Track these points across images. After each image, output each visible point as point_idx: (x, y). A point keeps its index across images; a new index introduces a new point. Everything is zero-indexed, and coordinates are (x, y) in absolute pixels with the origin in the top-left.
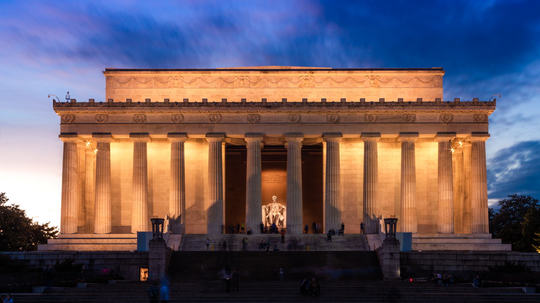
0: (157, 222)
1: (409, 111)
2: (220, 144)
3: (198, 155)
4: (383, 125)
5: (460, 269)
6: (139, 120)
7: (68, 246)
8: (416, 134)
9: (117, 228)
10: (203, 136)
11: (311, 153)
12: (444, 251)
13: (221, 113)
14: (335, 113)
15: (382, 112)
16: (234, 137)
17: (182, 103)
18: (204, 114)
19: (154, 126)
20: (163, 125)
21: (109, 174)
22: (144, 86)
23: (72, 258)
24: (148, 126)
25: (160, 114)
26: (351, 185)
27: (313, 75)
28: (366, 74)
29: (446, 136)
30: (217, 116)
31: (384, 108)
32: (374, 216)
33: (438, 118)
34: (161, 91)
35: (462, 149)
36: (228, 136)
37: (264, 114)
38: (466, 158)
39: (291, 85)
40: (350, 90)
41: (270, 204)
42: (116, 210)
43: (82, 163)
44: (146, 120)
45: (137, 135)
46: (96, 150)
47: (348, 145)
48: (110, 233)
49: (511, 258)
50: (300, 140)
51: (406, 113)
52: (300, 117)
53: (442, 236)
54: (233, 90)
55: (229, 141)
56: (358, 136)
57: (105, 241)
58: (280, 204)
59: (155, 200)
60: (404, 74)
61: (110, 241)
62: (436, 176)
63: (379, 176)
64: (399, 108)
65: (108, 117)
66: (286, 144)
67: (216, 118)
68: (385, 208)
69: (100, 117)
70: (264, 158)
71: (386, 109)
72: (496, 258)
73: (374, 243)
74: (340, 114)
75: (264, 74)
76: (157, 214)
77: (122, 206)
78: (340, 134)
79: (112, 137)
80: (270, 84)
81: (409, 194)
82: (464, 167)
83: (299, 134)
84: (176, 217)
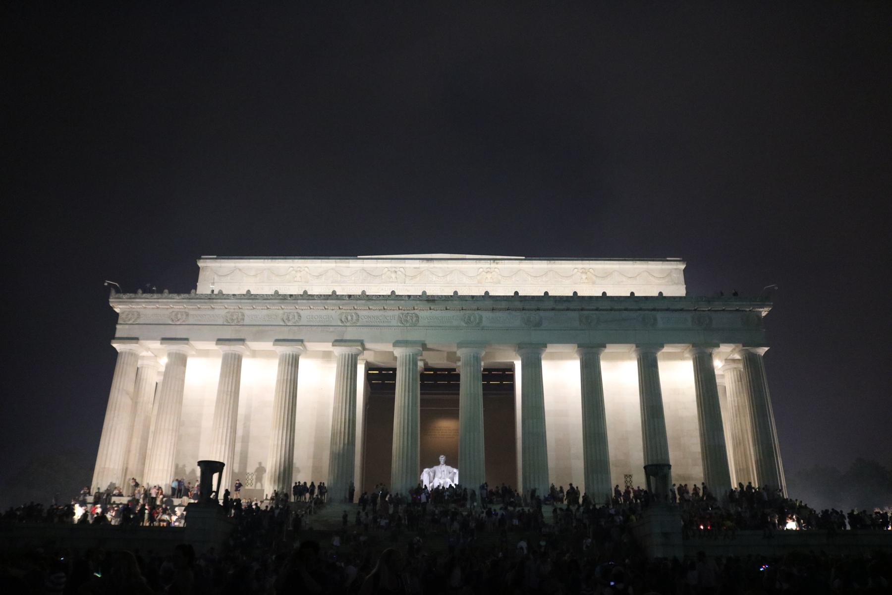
10: (328, 347)
13: (358, 312)
18: (333, 313)
19: (255, 329)
25: (265, 312)
28: (574, 266)
30: (352, 316)
36: (368, 345)
37: (425, 314)
41: (435, 468)
52: (481, 318)
55: (369, 356)
58: (449, 467)
65: (187, 315)
67: (349, 318)
69: (176, 315)
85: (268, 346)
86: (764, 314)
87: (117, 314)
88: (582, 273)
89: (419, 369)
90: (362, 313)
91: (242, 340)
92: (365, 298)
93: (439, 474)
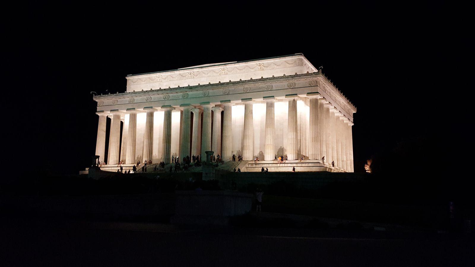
1: (269, 84)
6: (131, 101)
13: (169, 94)
15: (252, 85)
18: (161, 96)
22: (143, 83)
24: (135, 104)
27: (227, 67)
29: (291, 97)
30: (167, 96)
39: (215, 74)
52: (209, 92)
65: (117, 101)
67: (166, 97)
78: (229, 101)
80: (204, 75)
83: (208, 103)
85: (142, 110)
87: (97, 102)
90: (171, 95)
91: (134, 109)
92: (170, 89)
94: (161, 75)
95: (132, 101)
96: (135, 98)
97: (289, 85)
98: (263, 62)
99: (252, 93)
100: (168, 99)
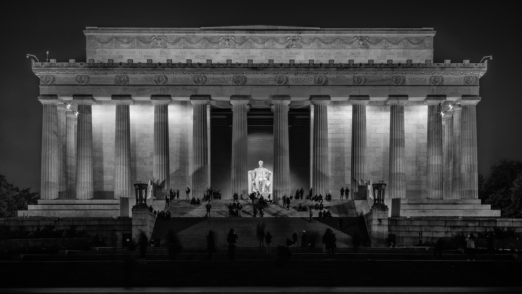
0: (140, 188)
2: (204, 107)
3: (181, 118)
4: (373, 88)
5: (449, 235)
6: (121, 81)
7: (49, 213)
8: (406, 96)
9: (99, 193)
10: (187, 99)
11: (298, 117)
12: (433, 217)
13: (205, 75)
14: (323, 75)
15: (370, 74)
16: (219, 99)
17: (165, 64)
18: (188, 76)
19: (137, 88)
20: (146, 87)
21: (91, 138)
23: (53, 224)
25: (143, 76)
26: (338, 150)
27: (301, 35)
28: (355, 35)
31: (373, 70)
32: (362, 181)
33: (428, 80)
34: (144, 51)
35: (453, 113)
36: (213, 98)
37: (251, 76)
38: (456, 122)
39: (278, 46)
40: (339, 51)
41: (256, 170)
42: (98, 173)
43: (62, 127)
44: (128, 81)
45: (119, 98)
46: (78, 113)
47: (336, 108)
48: (92, 199)
49: (500, 224)
50: (287, 102)
51: (395, 75)
52: (287, 79)
53: (431, 201)
54: (218, 50)
55: (213, 103)
56: (346, 99)
57: (87, 207)
59: (138, 165)
60: (394, 35)
61: (92, 207)
62: (425, 141)
63: (368, 141)
64: (388, 70)
65: (89, 78)
66: (273, 107)
67: (200, 79)
68: (373, 173)
69: (81, 78)
70: (250, 121)
71: (375, 71)
72: (486, 224)
73: (362, 208)
74: (328, 76)
75: (250, 35)
76: (140, 180)
77: (104, 170)
79: (93, 99)
81: (398, 159)
82: (454, 131)
84: (161, 181)
86: (481, 74)
88: (360, 40)
89: (247, 110)
93: (258, 175)
94: (165, 34)
95: (122, 79)
96: (130, 76)
97: (433, 79)
98: (367, 35)
99: (370, 88)
100: (204, 83)
